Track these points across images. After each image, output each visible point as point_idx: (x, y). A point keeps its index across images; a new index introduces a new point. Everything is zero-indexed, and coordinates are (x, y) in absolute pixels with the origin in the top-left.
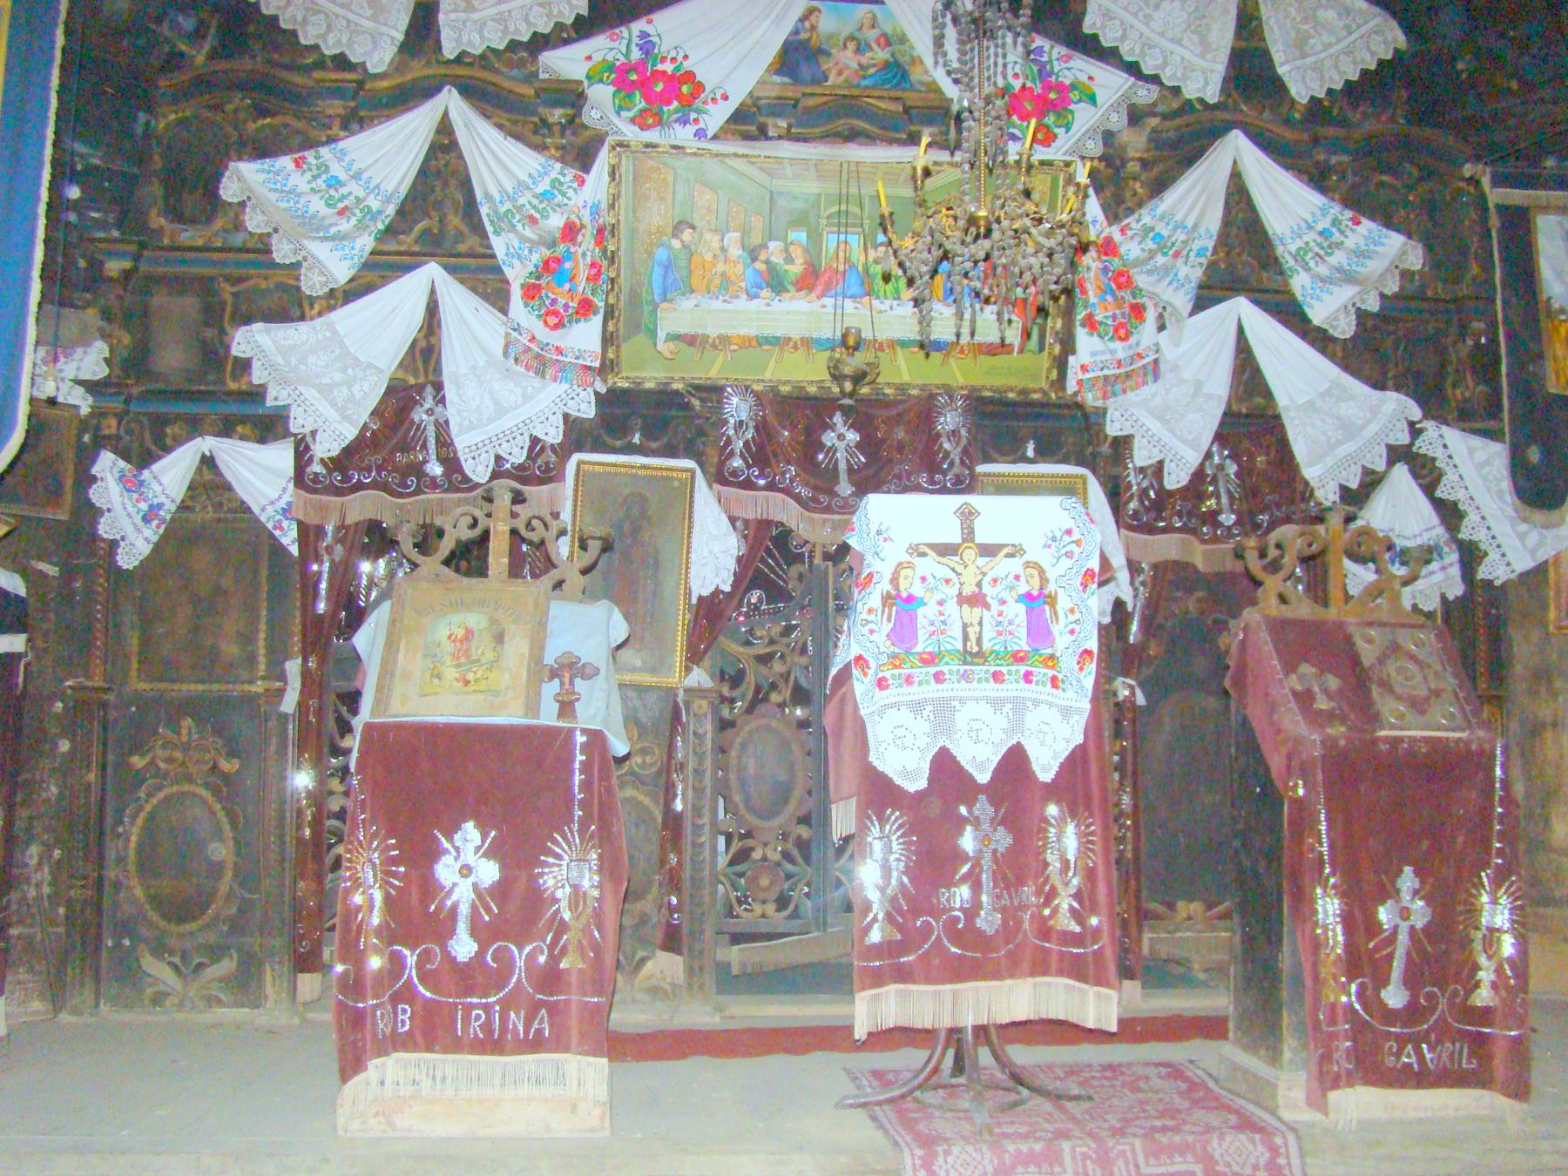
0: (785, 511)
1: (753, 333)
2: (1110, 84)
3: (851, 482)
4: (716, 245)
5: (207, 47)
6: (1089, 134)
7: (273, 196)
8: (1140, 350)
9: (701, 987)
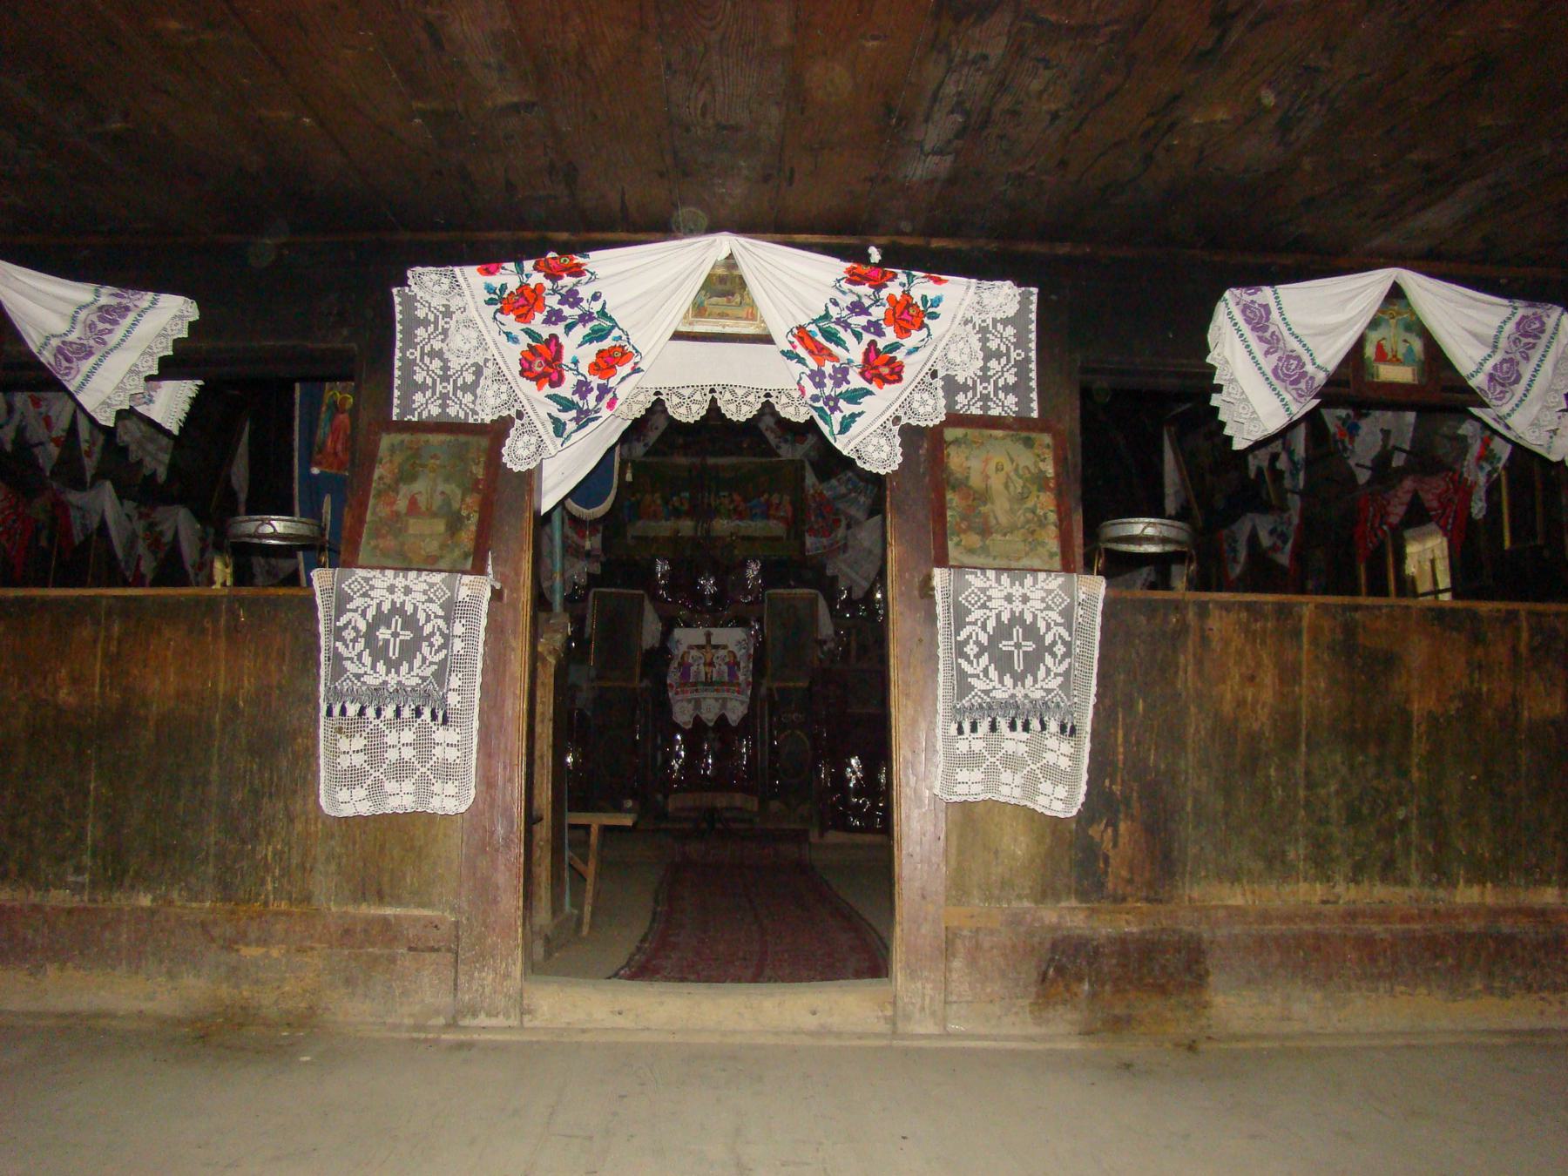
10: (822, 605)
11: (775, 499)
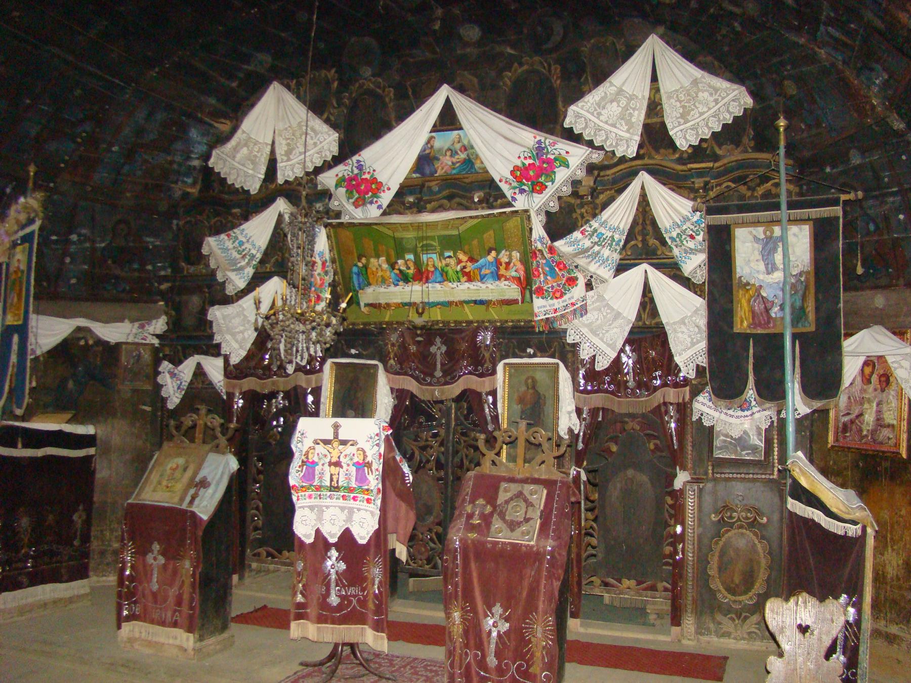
0: (410, 385)
1: (400, 301)
2: (577, 155)
3: (442, 370)
4: (376, 264)
5: (198, 187)
6: (564, 183)
7: (219, 252)
8: (573, 301)
10: (564, 374)
11: (504, 257)
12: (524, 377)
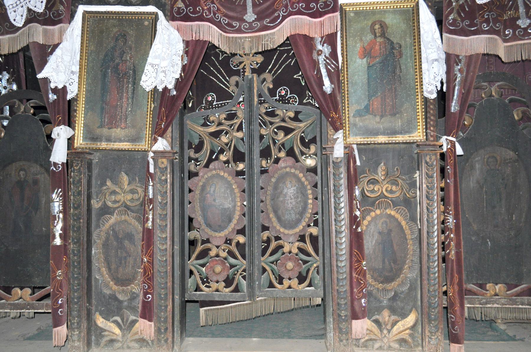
9: (166, 341)
12: (370, 23)
